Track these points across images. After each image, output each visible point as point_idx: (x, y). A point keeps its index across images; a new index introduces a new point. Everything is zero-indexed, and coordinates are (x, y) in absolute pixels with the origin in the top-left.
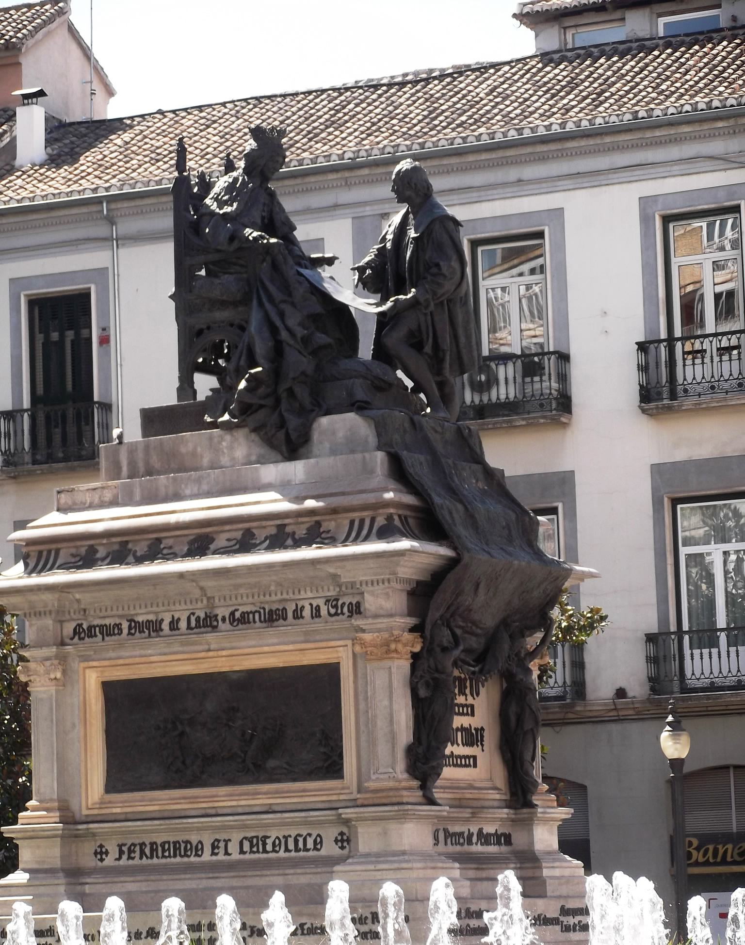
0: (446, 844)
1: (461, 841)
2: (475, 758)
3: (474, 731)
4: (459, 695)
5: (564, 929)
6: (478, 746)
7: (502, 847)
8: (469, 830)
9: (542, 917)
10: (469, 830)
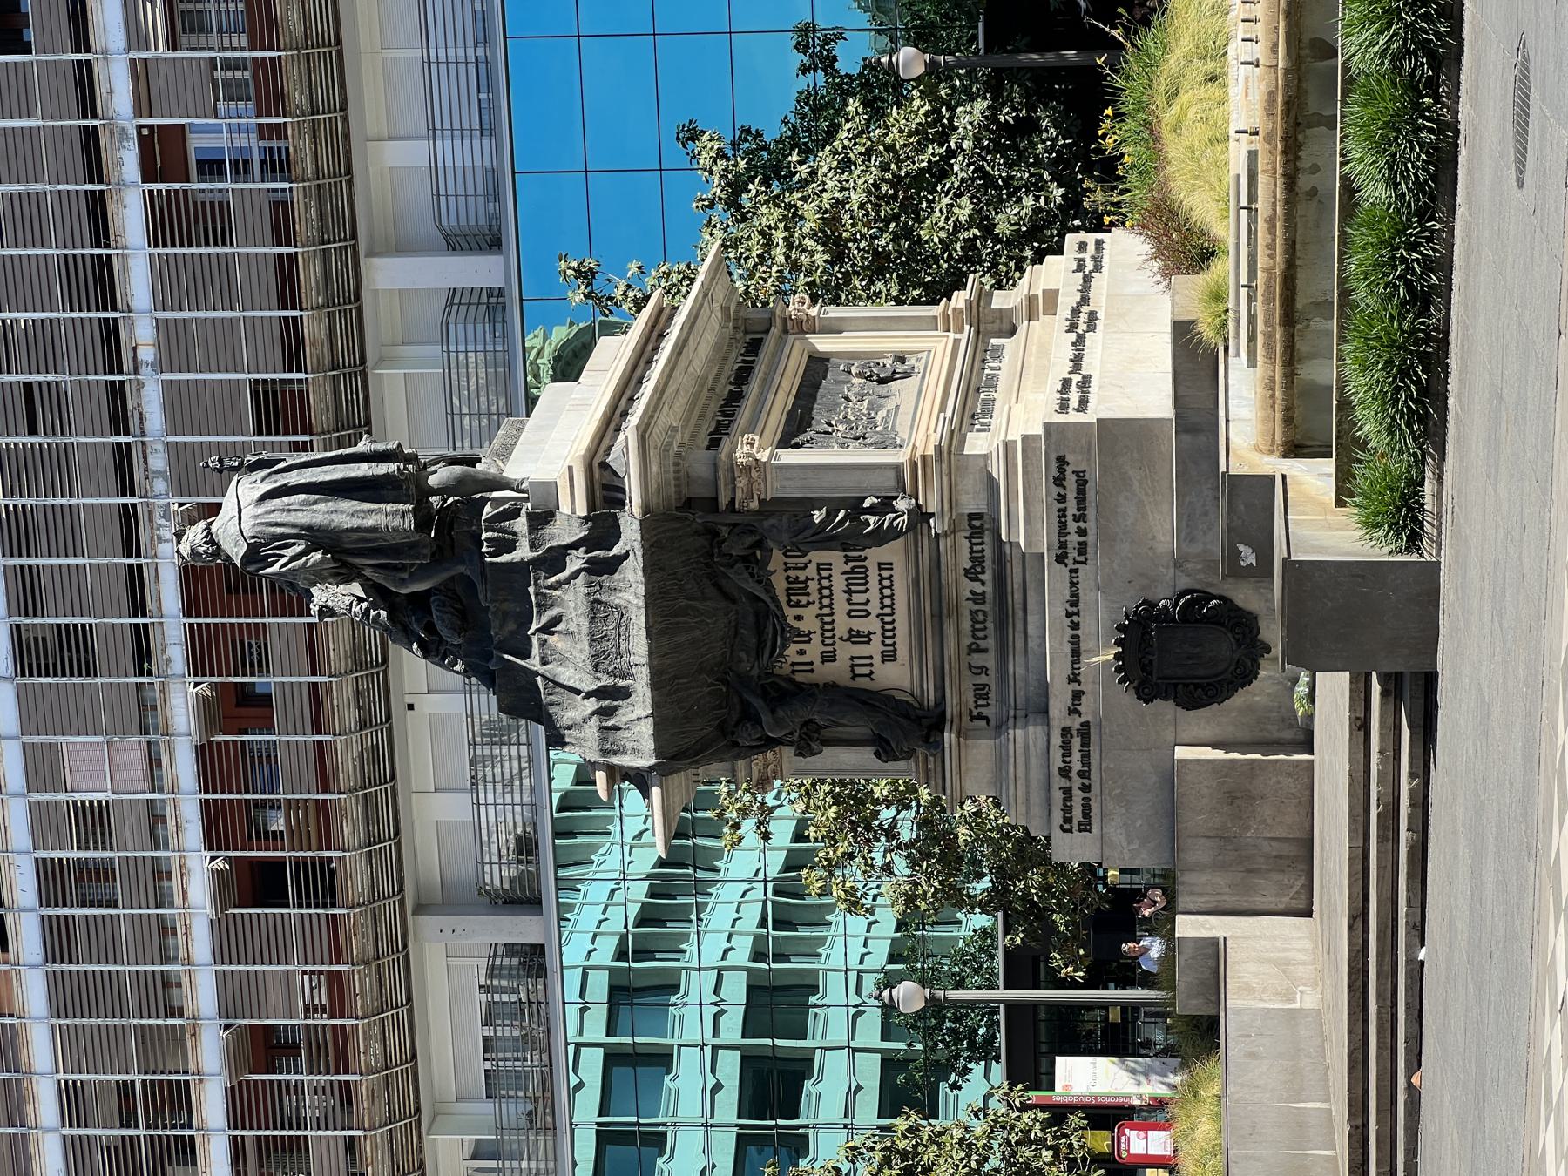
0: (985, 651)
1: (981, 617)
2: (881, 566)
3: (848, 568)
4: (808, 594)
5: (1082, 558)
6: (866, 558)
7: (986, 526)
8: (968, 599)
9: (1068, 606)
10: (968, 599)
